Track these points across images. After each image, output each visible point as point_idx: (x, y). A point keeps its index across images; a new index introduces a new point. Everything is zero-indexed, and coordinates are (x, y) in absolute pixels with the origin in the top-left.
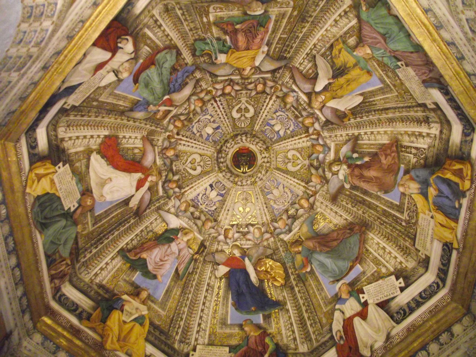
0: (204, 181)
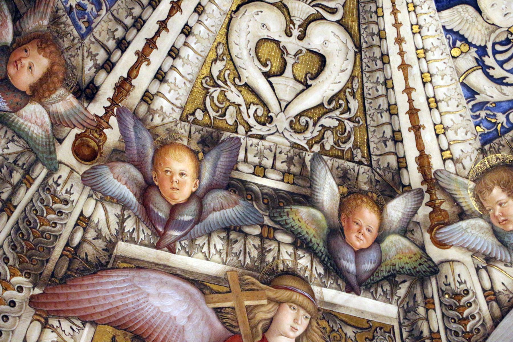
0: (405, 32)
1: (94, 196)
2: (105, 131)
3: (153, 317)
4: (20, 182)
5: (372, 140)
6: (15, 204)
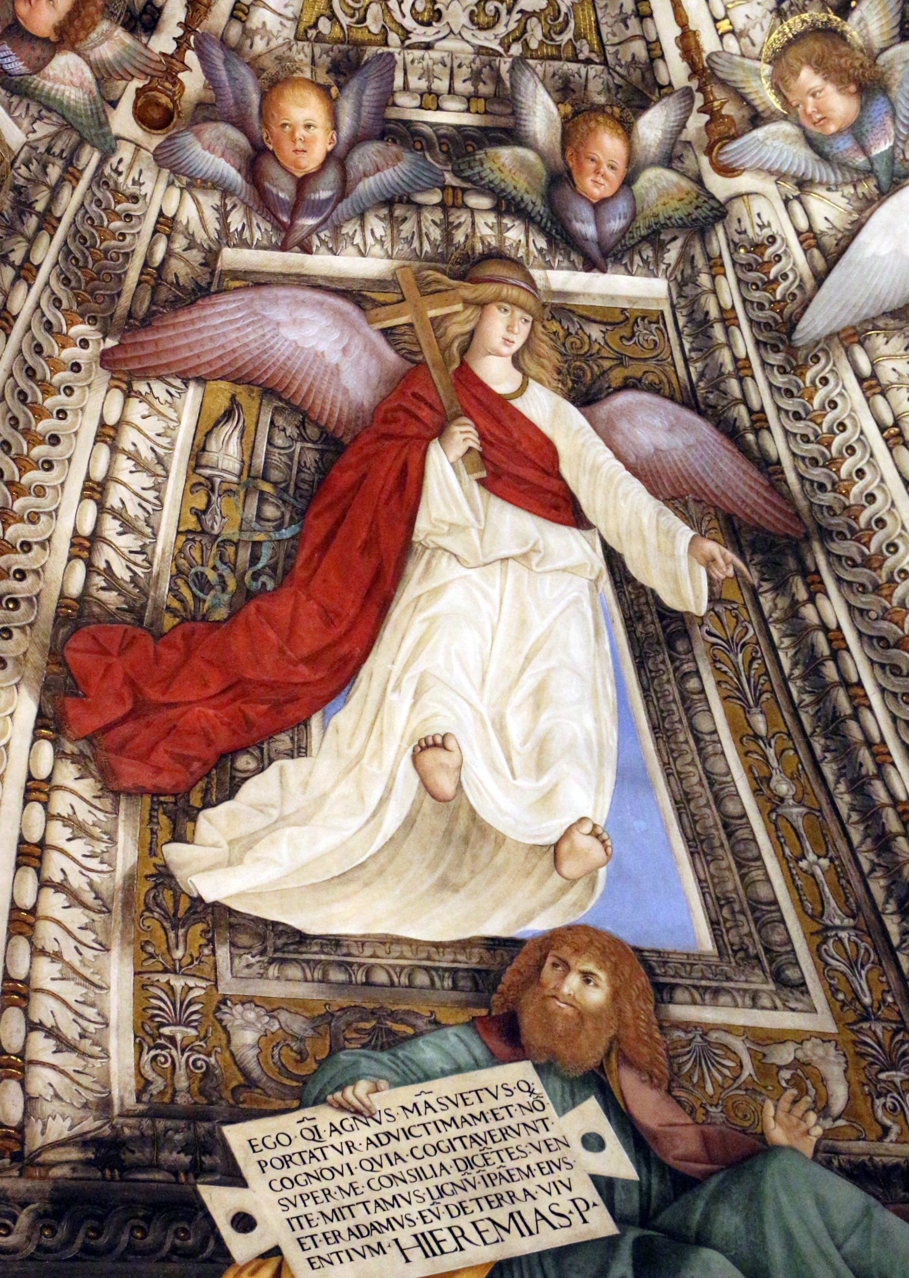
1: (177, 183)
2: (181, 76)
3: (289, 358)
4: (61, 180)
5: (603, 21)
6: (58, 214)
